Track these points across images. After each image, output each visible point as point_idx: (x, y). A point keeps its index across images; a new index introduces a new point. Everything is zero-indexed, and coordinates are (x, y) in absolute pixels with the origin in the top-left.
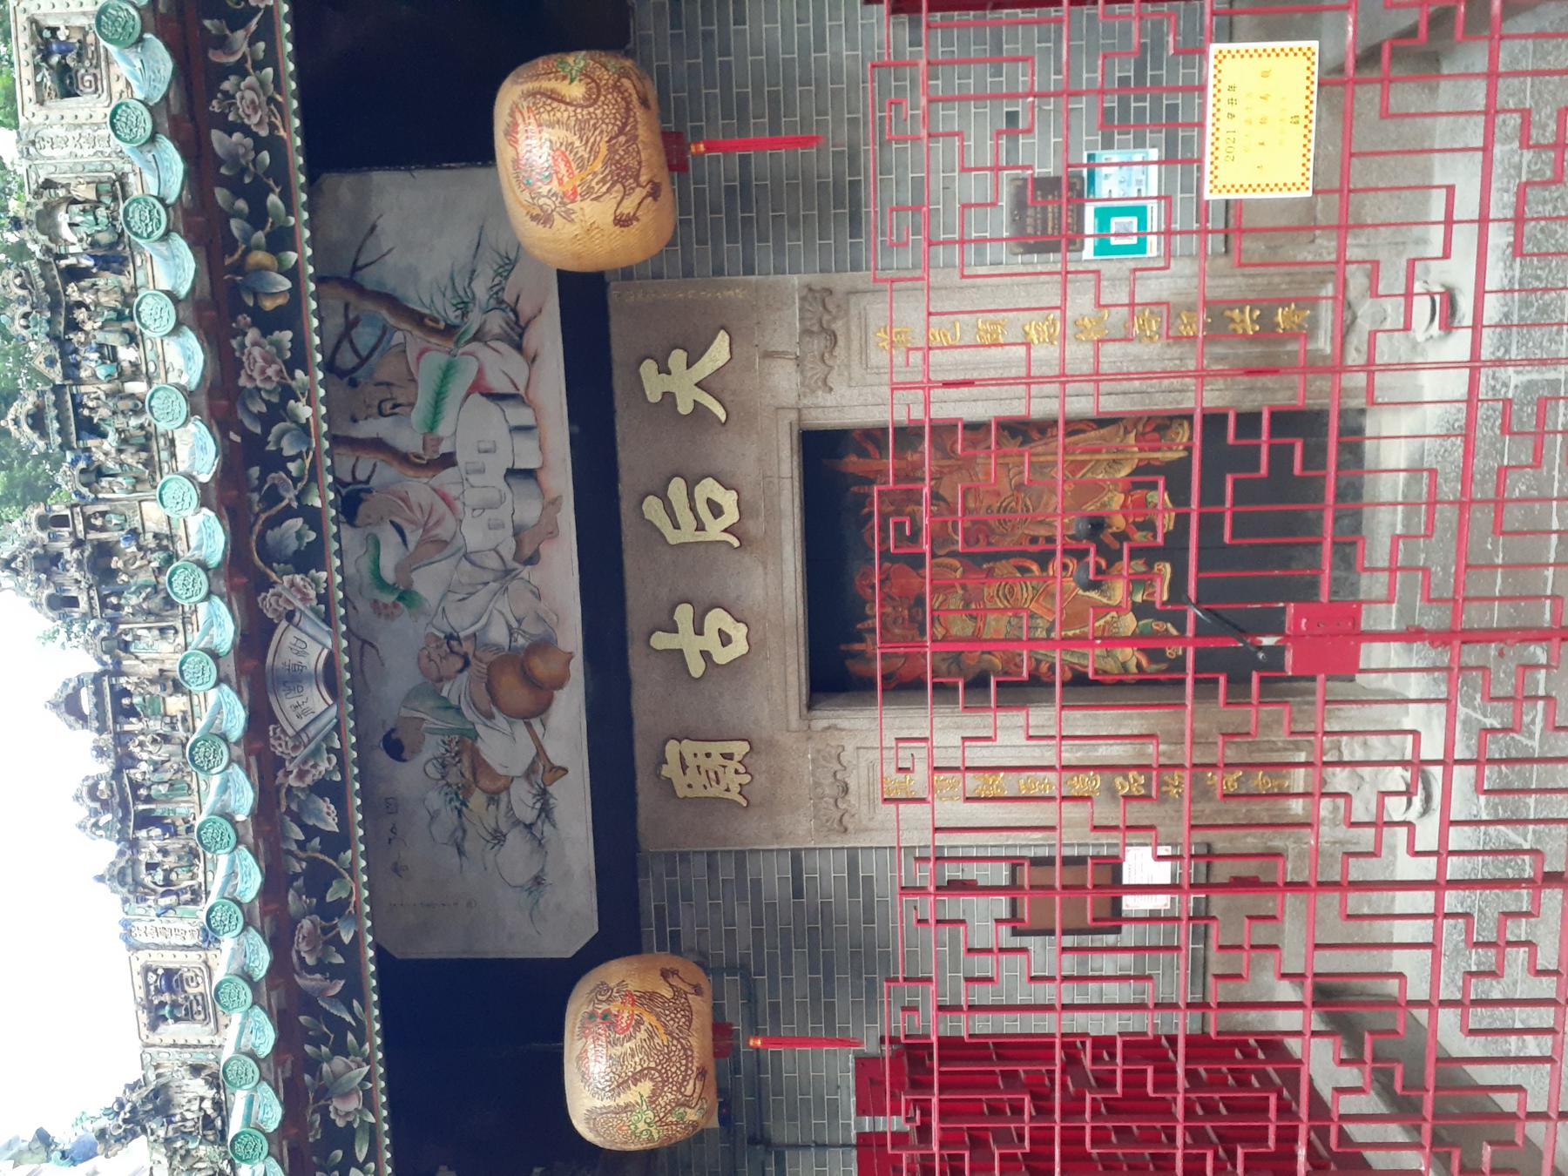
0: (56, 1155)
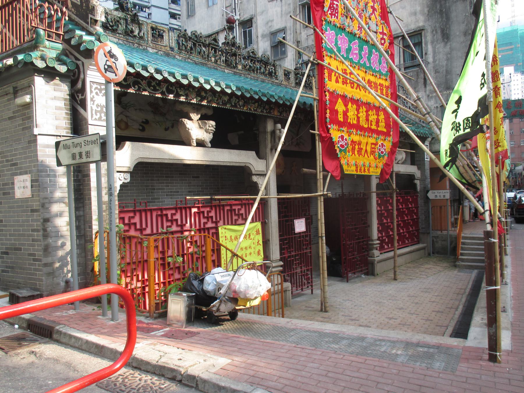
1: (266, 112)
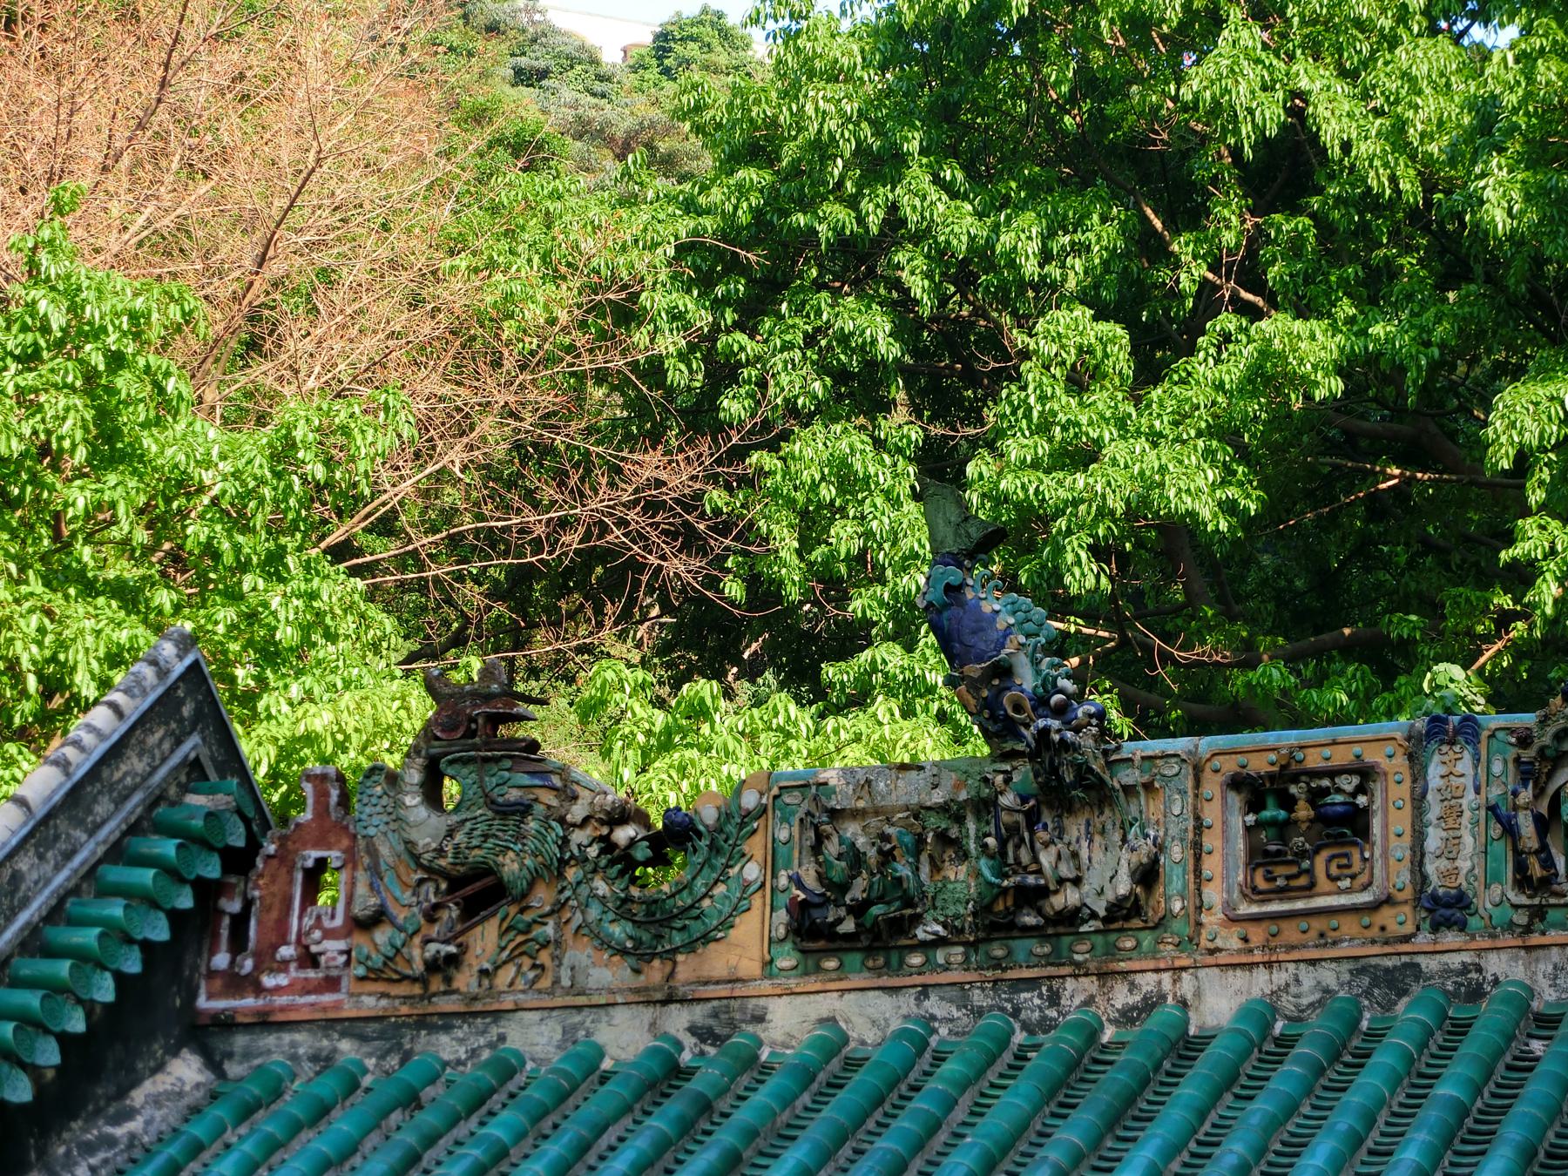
0: (954, 575)
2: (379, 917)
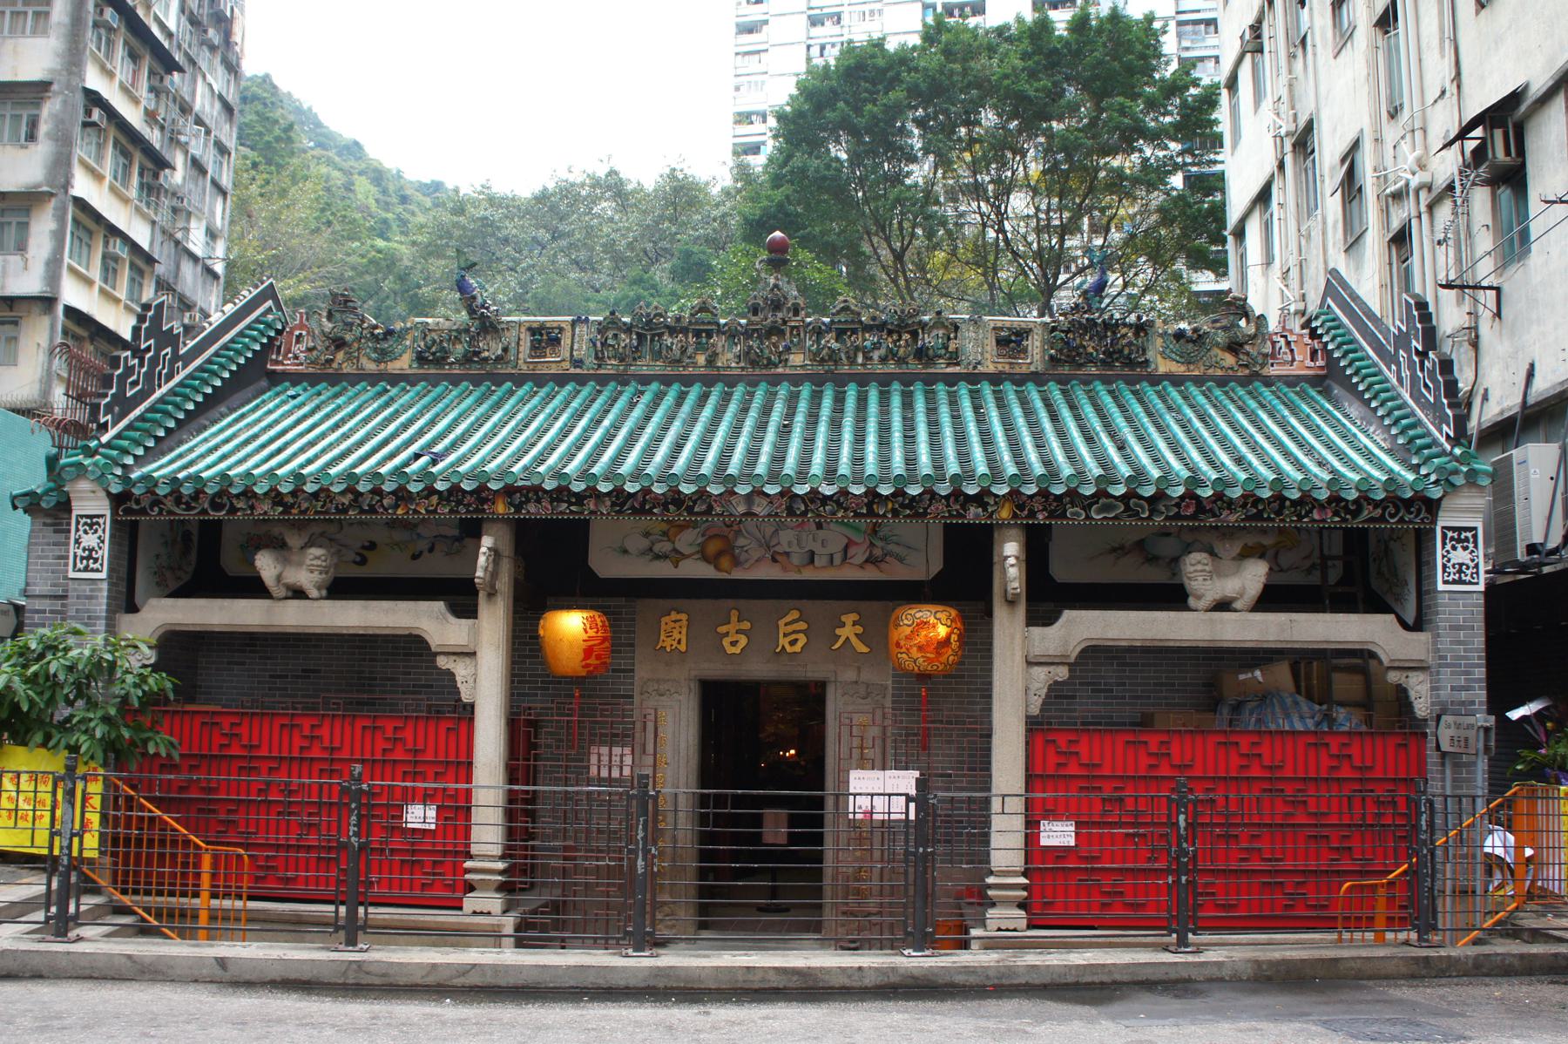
1: (468, 512)
2: (314, 348)
